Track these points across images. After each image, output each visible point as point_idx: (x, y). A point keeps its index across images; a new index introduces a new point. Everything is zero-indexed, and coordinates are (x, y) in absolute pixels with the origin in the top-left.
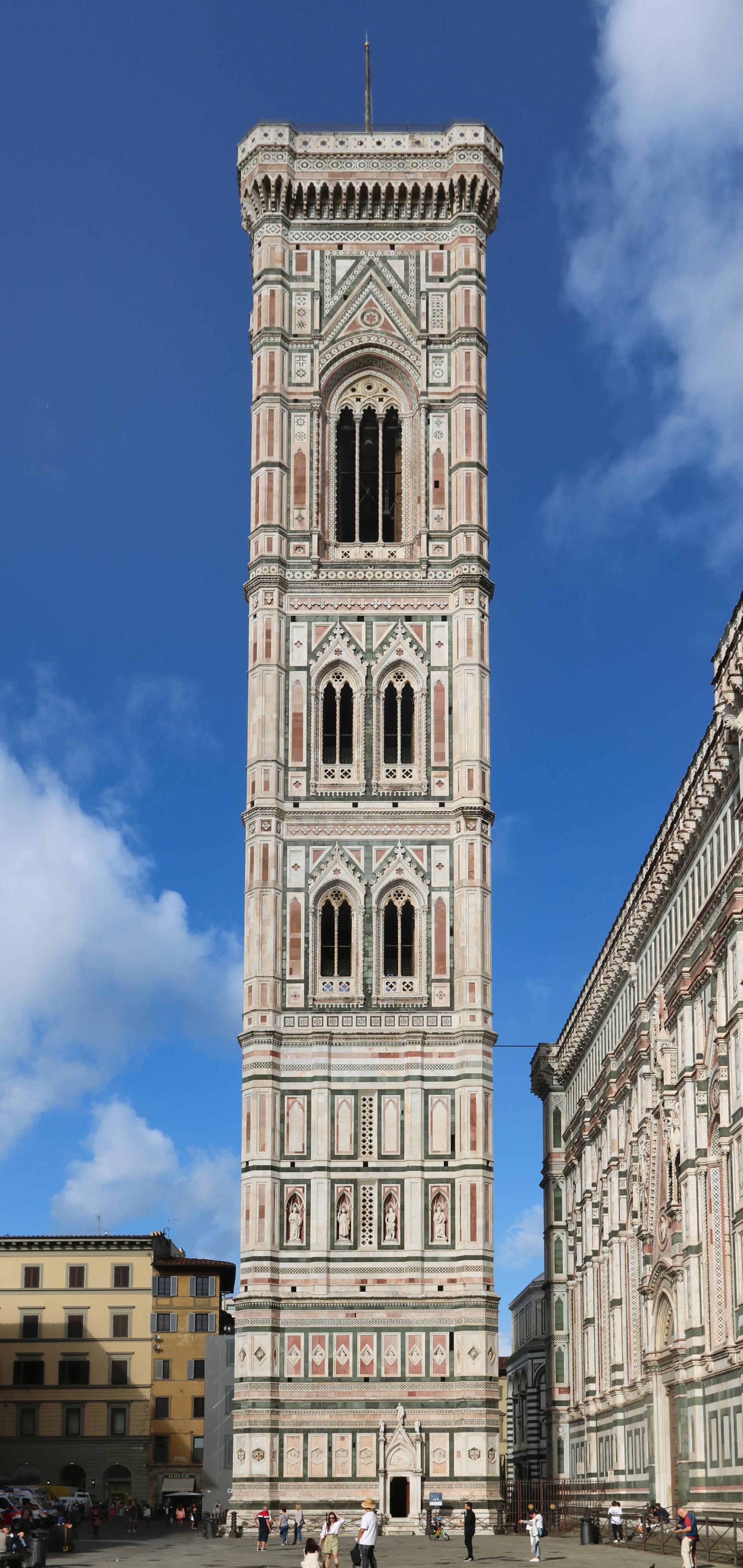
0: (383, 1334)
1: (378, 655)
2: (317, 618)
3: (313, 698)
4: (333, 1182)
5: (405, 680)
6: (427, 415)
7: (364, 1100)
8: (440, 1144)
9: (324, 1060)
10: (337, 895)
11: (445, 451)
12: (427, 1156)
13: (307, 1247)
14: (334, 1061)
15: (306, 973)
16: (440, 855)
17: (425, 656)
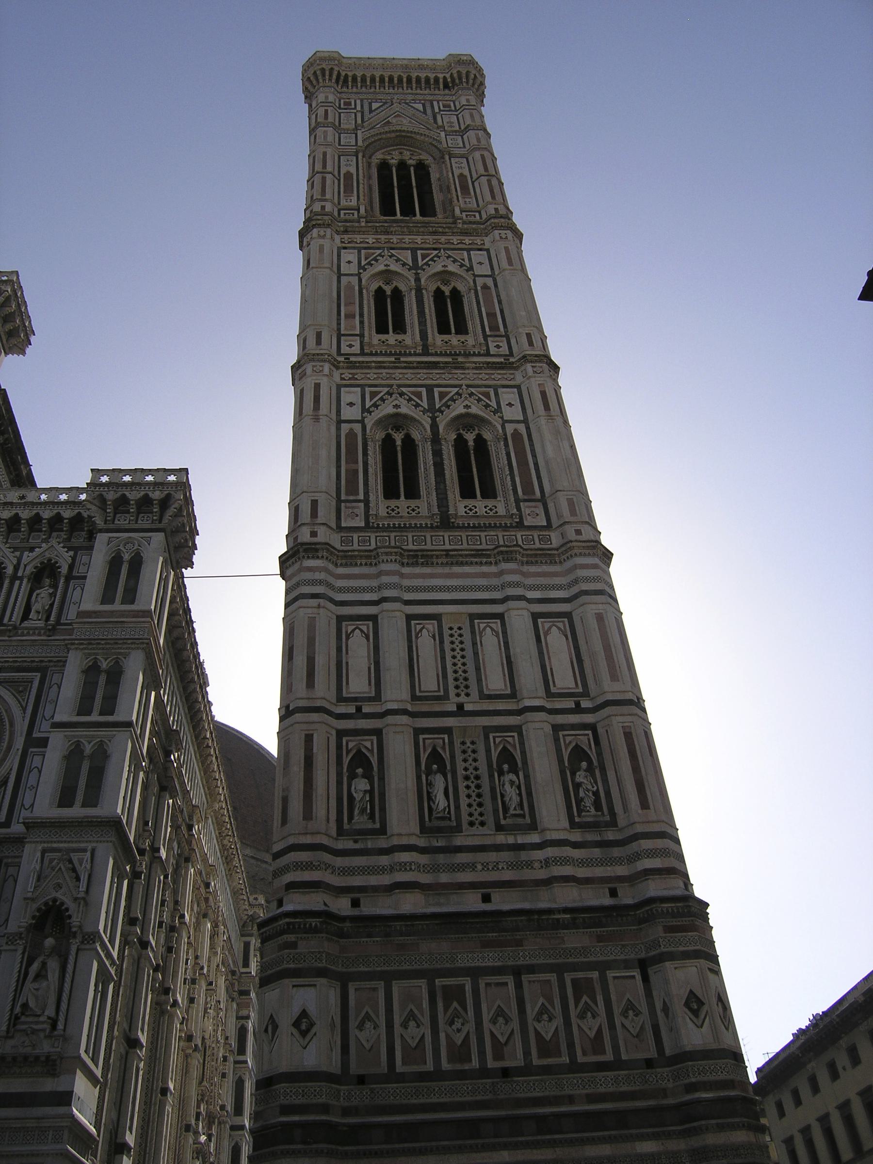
0: (525, 978)
1: (424, 267)
2: (365, 248)
3: (364, 291)
4: (418, 732)
5: (451, 287)
6: (450, 159)
7: (451, 629)
8: (564, 679)
9: (395, 579)
10: (398, 430)
11: (466, 172)
12: (549, 694)
13: (382, 831)
14: (406, 582)
15: (366, 493)
16: (508, 396)
17: (471, 268)
